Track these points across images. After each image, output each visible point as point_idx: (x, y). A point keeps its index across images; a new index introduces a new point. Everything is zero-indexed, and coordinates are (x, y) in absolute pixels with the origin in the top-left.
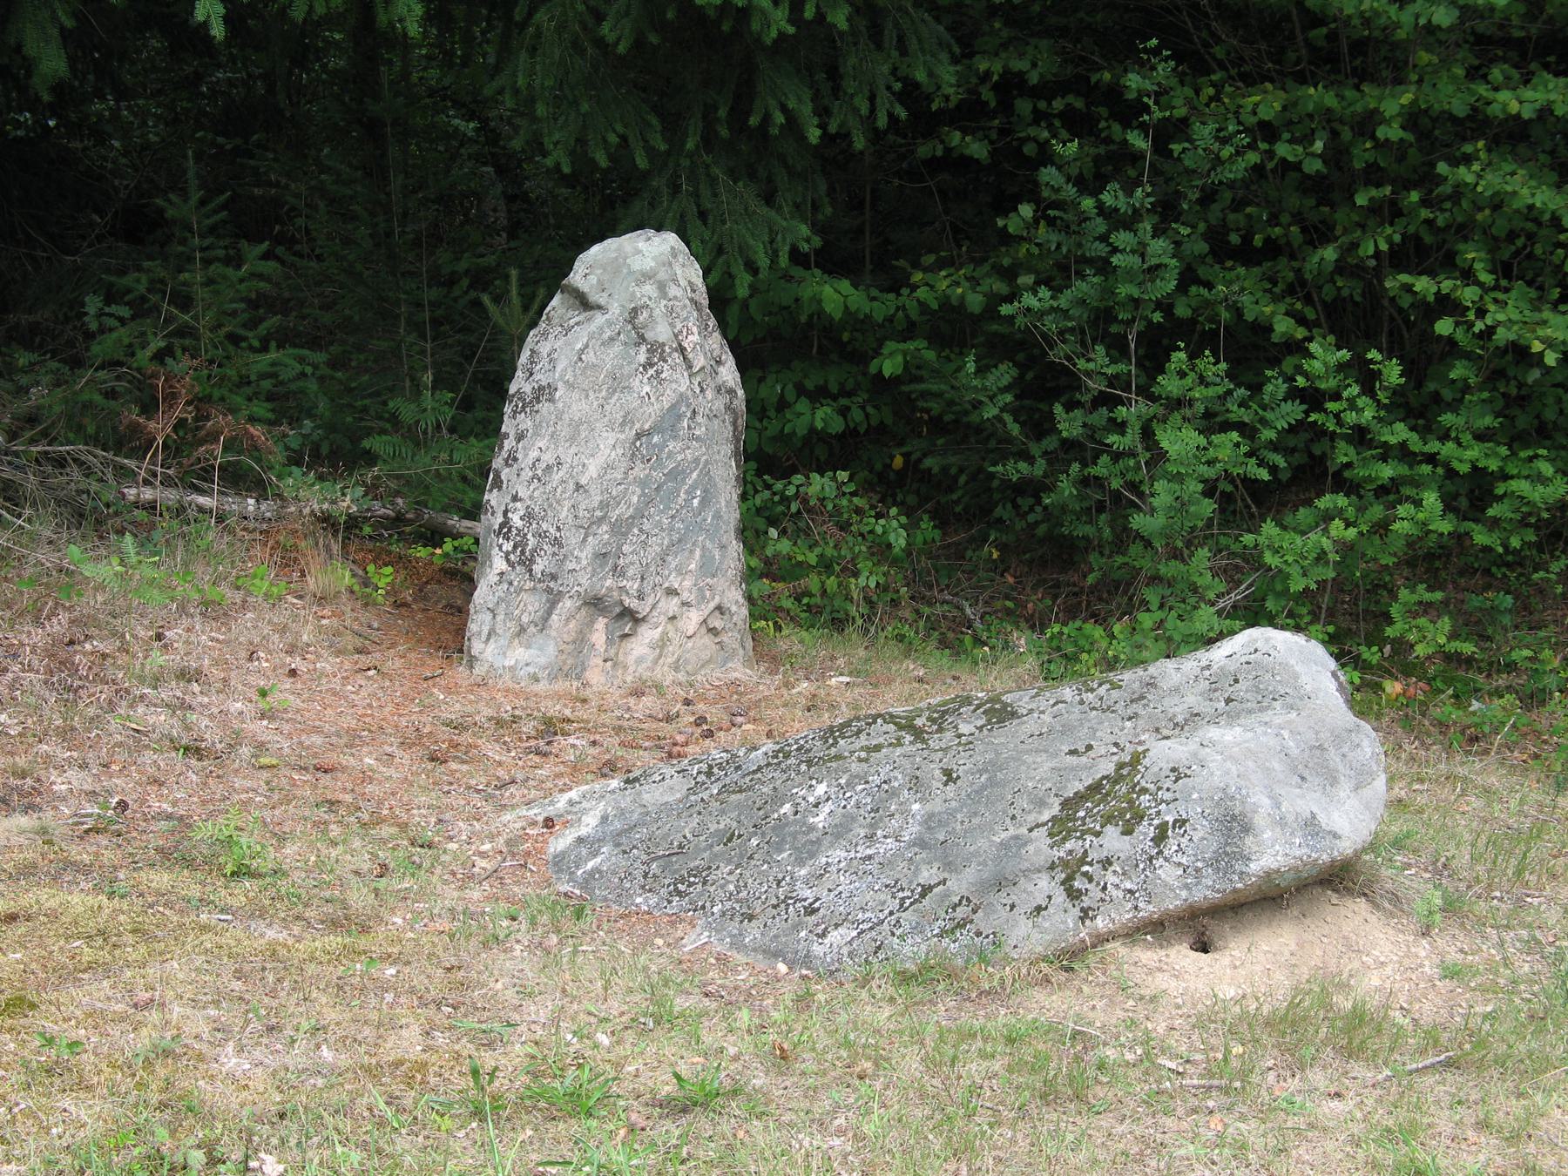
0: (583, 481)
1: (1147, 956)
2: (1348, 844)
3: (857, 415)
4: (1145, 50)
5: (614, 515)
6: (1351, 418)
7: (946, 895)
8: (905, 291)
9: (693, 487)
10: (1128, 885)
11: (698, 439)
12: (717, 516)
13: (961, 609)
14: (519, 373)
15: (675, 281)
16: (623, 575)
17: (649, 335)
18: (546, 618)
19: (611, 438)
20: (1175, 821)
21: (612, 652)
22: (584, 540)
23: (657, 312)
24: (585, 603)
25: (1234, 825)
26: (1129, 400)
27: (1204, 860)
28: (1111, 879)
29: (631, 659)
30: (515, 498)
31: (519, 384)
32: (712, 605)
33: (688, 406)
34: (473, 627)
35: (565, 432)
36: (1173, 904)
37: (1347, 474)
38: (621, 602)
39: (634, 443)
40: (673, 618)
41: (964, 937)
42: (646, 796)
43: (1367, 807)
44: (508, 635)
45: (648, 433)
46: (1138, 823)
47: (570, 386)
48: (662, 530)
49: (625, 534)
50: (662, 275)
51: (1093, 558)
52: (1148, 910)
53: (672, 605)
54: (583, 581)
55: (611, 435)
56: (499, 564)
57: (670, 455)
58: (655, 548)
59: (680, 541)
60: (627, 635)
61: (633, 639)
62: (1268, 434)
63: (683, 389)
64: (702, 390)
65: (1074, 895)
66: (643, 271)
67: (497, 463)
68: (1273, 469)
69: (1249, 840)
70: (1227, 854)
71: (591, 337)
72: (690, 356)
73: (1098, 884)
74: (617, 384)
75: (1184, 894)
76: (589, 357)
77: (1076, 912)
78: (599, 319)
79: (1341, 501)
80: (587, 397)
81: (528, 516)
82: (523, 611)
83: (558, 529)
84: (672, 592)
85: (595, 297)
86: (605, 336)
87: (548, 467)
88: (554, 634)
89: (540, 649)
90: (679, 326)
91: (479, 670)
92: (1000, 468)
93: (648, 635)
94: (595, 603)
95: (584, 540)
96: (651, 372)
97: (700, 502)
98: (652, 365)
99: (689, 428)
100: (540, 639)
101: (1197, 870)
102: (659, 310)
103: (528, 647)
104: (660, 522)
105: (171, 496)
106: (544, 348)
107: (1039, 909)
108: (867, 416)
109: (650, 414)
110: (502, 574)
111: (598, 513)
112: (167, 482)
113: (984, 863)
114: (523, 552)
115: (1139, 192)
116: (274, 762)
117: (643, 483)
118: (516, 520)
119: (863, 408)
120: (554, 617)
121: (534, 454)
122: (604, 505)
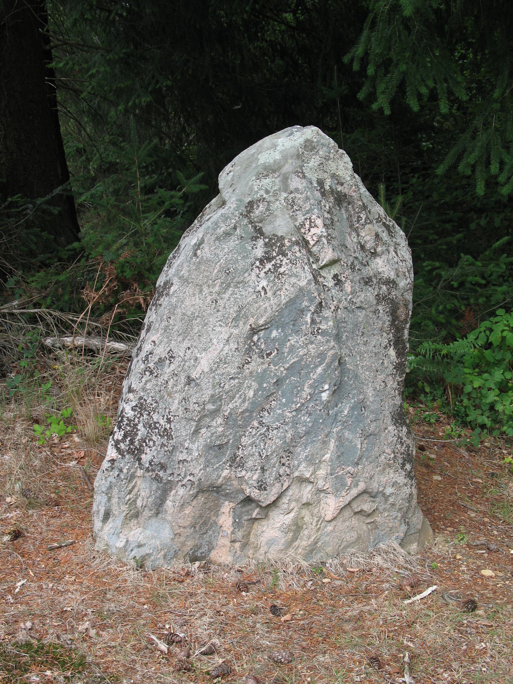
0: (194, 375)
5: (227, 409)
9: (321, 380)
11: (324, 333)
16: (241, 465)
17: (267, 229)
19: (224, 332)
21: (239, 535)
22: (196, 432)
23: (274, 206)
29: (263, 539)
32: (354, 492)
33: (311, 300)
38: (242, 491)
39: (250, 337)
45: (266, 327)
47: (185, 281)
48: (285, 423)
53: (306, 492)
57: (292, 349)
58: (276, 440)
61: (264, 523)
63: (303, 283)
71: (206, 233)
72: (315, 249)
74: (230, 278)
76: (205, 252)
80: (201, 291)
81: (140, 407)
83: (169, 421)
84: (302, 480)
86: (223, 228)
87: (161, 361)
88: (169, 518)
90: (301, 218)
91: (100, 546)
95: (196, 432)
96: (269, 266)
98: (269, 259)
99: (313, 321)
104: (282, 415)
109: (267, 308)
110: (113, 461)
111: (210, 407)
114: (132, 442)
117: (261, 378)
120: (169, 503)
122: (213, 399)
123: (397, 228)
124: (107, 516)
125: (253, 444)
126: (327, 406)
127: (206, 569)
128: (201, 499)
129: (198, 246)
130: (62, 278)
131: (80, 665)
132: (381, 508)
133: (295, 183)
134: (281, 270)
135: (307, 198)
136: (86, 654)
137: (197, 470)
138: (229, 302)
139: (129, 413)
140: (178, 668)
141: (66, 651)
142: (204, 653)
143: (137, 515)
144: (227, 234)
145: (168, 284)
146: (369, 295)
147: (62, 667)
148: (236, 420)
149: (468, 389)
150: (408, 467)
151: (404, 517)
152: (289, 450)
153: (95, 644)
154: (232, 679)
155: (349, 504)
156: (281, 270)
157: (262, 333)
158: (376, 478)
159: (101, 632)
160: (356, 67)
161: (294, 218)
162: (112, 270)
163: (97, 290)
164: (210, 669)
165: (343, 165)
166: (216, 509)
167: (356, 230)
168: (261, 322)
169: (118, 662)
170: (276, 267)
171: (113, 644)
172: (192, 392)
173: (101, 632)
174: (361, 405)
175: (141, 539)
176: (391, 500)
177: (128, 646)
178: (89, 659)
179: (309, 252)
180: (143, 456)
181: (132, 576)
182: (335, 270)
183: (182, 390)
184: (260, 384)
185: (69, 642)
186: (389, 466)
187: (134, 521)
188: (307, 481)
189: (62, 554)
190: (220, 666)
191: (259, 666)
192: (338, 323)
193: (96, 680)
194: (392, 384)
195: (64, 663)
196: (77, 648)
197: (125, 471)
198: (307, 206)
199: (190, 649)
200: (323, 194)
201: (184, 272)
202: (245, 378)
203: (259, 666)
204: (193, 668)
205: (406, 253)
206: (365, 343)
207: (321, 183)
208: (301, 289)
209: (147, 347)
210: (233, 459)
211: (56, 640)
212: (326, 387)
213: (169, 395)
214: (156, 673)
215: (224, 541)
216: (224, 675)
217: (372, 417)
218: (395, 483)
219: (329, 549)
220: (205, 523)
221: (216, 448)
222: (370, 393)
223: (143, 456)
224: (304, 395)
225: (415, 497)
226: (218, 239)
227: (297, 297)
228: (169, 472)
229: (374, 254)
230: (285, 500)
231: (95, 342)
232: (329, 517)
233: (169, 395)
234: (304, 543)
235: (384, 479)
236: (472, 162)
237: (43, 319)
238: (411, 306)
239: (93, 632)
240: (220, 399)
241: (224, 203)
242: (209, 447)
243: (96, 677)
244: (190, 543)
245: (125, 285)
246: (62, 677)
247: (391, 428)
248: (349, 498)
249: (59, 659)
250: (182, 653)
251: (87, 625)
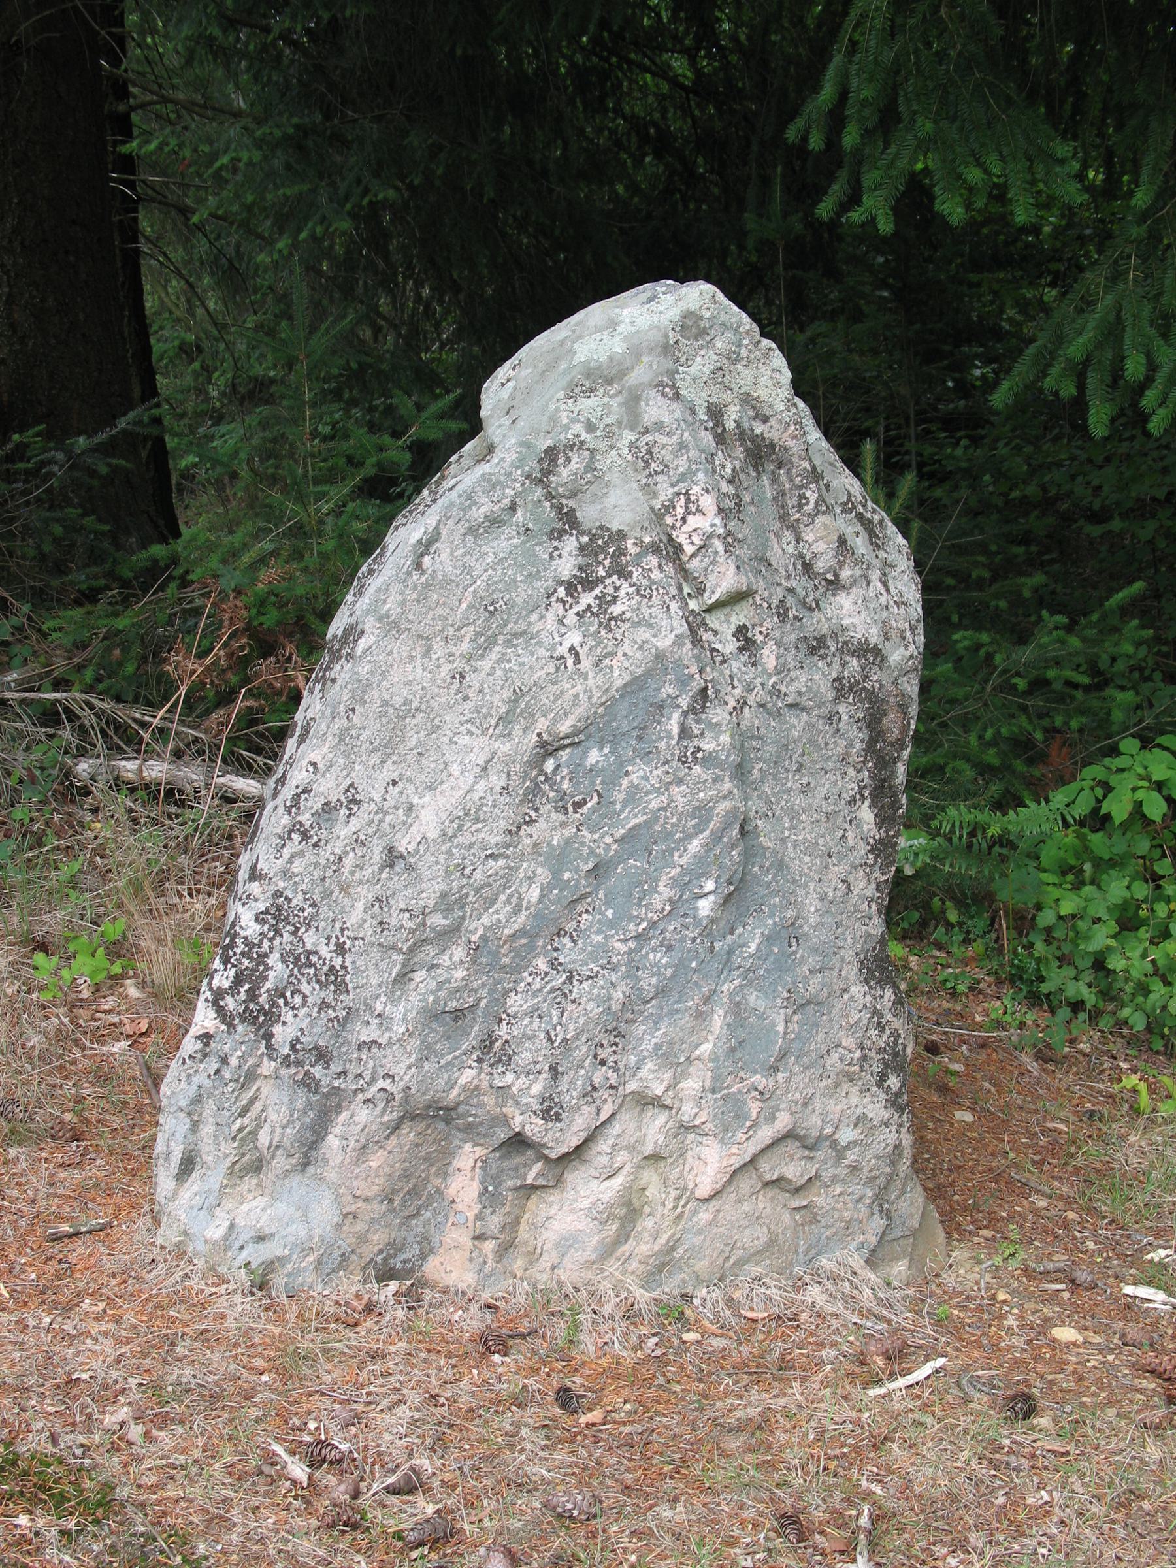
0: (403, 845)
5: (476, 928)
9: (699, 870)
16: (505, 1060)
17: (588, 514)
18: (314, 1145)
19: (477, 749)
21: (494, 1222)
22: (403, 977)
23: (602, 462)
24: (409, 1116)
29: (549, 1236)
32: (766, 1134)
33: (683, 682)
35: (372, 730)
38: (505, 1120)
40: (655, 1158)
45: (576, 740)
47: (392, 626)
48: (610, 966)
49: (515, 970)
53: (654, 1130)
55: (479, 742)
58: (586, 1006)
59: (661, 992)
61: (553, 1197)
63: (664, 642)
72: (695, 565)
74: (497, 623)
76: (442, 561)
80: (428, 651)
81: (276, 915)
83: (341, 950)
84: (645, 1102)
86: (484, 508)
88: (332, 1176)
91: (168, 1235)
93: (589, 1192)
95: (403, 977)
96: (587, 599)
98: (589, 583)
99: (685, 732)
110: (206, 1038)
111: (438, 920)
114: (252, 995)
117: (559, 858)
120: (333, 1141)
122: (446, 903)
123: (891, 528)
124: (188, 1165)
125: (534, 1012)
126: (709, 931)
127: (411, 1298)
128: (408, 1134)
129: (426, 546)
130: (122, 623)
131: (100, 1504)
132: (826, 1176)
133: (657, 409)
134: (616, 610)
135: (682, 446)
136: (116, 1481)
137: (402, 1067)
138: (492, 678)
139: (250, 927)
140: (329, 1520)
141: (70, 1471)
142: (393, 1490)
143: (257, 1167)
144: (494, 522)
145: (353, 633)
146: (817, 678)
147: (56, 1508)
148: (496, 955)
149: (1046, 918)
150: (893, 1082)
151: (879, 1198)
152: (616, 1029)
153: (140, 1459)
154: (454, 1552)
155: (753, 1161)
156: (616, 610)
157: (565, 755)
158: (817, 1103)
159: (155, 1432)
161: (649, 490)
162: (237, 611)
163: (202, 655)
164: (404, 1526)
165: (770, 375)
166: (442, 1160)
167: (794, 528)
168: (564, 728)
169: (191, 1501)
170: (604, 602)
171: (181, 1459)
172: (396, 883)
173: (155, 1432)
174: (789, 933)
175: (265, 1222)
176: (851, 1157)
177: (216, 1466)
178: (122, 1492)
179: (682, 570)
180: (277, 1029)
181: (238, 1308)
182: (741, 615)
184: (556, 873)
185: (78, 1452)
186: (850, 1078)
187: (250, 1181)
188: (657, 1103)
189: (79, 1250)
190: (427, 1521)
191: (519, 1525)
192: (743, 739)
193: (134, 1540)
195: (63, 1498)
196: (95, 1466)
197: (234, 1061)
198: (682, 465)
199: (362, 1479)
200: (720, 438)
201: (391, 606)
202: (522, 857)
203: (519, 1525)
204: (366, 1524)
206: (805, 790)
207: (716, 413)
208: (660, 656)
209: (298, 776)
210: (487, 1044)
211: (49, 1446)
212: (710, 885)
213: (345, 889)
214: (278, 1531)
215: (457, 1236)
216: (436, 1541)
217: (813, 961)
218: (862, 1117)
219: (701, 1266)
220: (414, 1192)
222: (811, 905)
223: (277, 1029)
224: (658, 901)
225: (907, 1153)
226: (471, 531)
227: (649, 673)
228: (336, 1068)
229: (834, 585)
230: (603, 1145)
231: (191, 774)
232: (703, 1191)
233: (345, 889)
234: (644, 1249)
235: (835, 1108)
237: (72, 716)
238: (914, 710)
239: (135, 1432)
240: (462, 902)
241: (491, 449)
242: (433, 1015)
243: (134, 1535)
244: (378, 1238)
245: (266, 646)
246: (54, 1532)
247: (858, 990)
248: (752, 1149)
249: (50, 1488)
250: (342, 1488)
251: (124, 1413)
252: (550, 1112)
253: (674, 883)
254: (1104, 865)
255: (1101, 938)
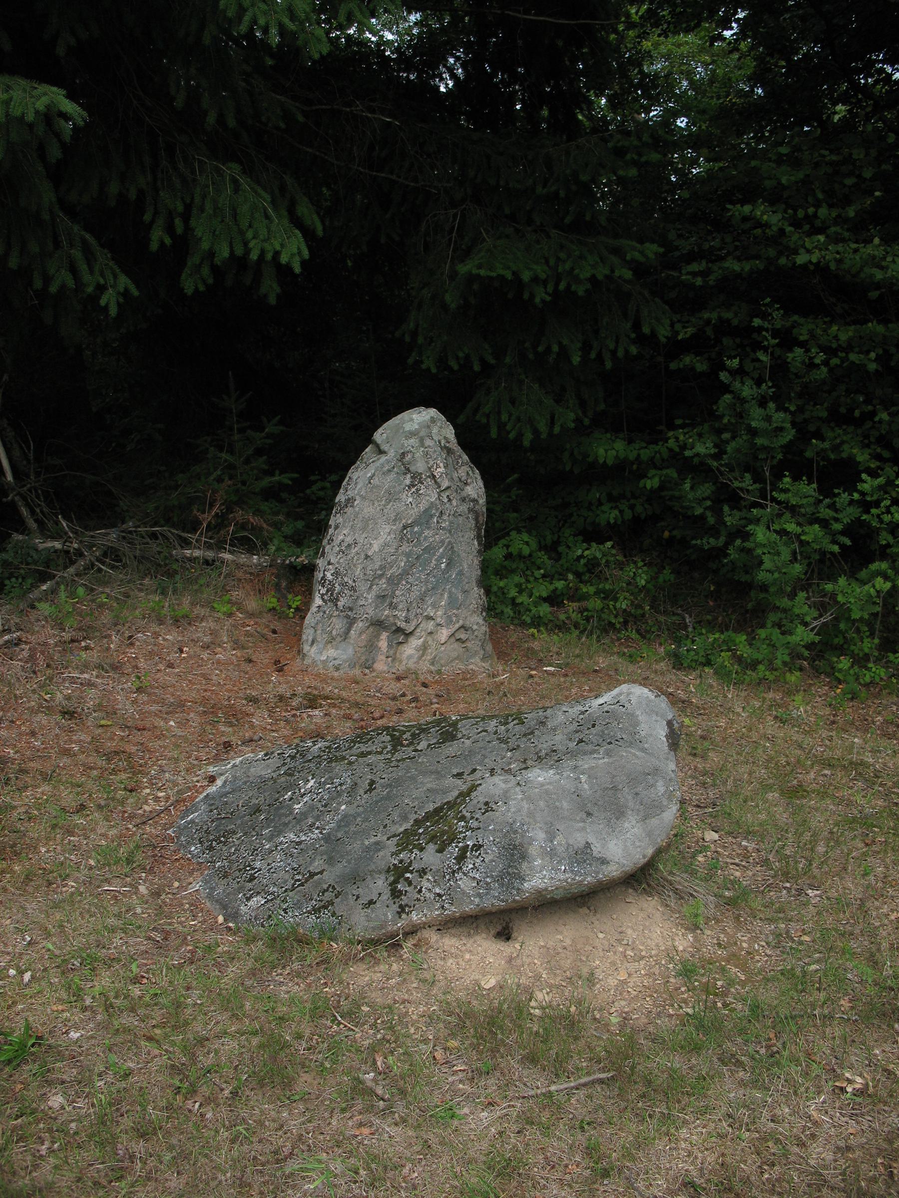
0: (370, 554)
1: (449, 942)
2: (614, 868)
3: (639, 509)
4: (765, 305)
5: (389, 573)
6: (887, 518)
7: (319, 883)
8: (661, 443)
9: (441, 557)
10: (438, 891)
12: (461, 573)
13: (684, 619)
14: (341, 491)
15: (430, 436)
16: (395, 608)
17: (412, 468)
20: (474, 845)
21: (391, 652)
22: (370, 587)
24: (372, 624)
25: (515, 853)
26: (767, 505)
27: (492, 877)
28: (426, 884)
29: (405, 656)
30: (329, 563)
31: (341, 497)
32: (457, 626)
33: (437, 509)
34: (304, 637)
36: (469, 908)
37: (888, 551)
38: (395, 624)
39: (402, 531)
40: (431, 633)
41: (325, 915)
42: (252, 770)
43: (649, 834)
44: (324, 642)
45: (411, 525)
46: (449, 844)
47: (363, 498)
48: (421, 582)
50: (422, 434)
51: (753, 593)
52: (452, 910)
53: (431, 625)
54: (370, 612)
56: (318, 601)
57: (426, 538)
58: (415, 593)
59: (433, 588)
60: (401, 643)
61: (405, 645)
62: (838, 527)
64: (450, 500)
65: (396, 894)
66: (418, 432)
67: (325, 542)
68: (842, 546)
69: (525, 865)
70: (509, 874)
73: (416, 887)
74: (391, 496)
75: (477, 900)
76: (376, 481)
77: (395, 908)
78: (383, 458)
79: (884, 566)
80: (373, 504)
81: (336, 574)
82: (333, 628)
83: (354, 581)
85: (384, 447)
86: (385, 469)
87: (349, 545)
88: (352, 642)
89: (344, 650)
92: (699, 542)
94: (378, 624)
95: (370, 587)
96: (413, 490)
97: (448, 565)
98: (414, 486)
99: (438, 522)
100: (343, 645)
101: (487, 884)
102: (419, 454)
103: (337, 649)
105: (210, 554)
106: (355, 478)
107: (371, 902)
108: (645, 509)
109: (414, 513)
110: (319, 607)
111: (379, 572)
112: (209, 547)
113: (349, 862)
114: (332, 595)
115: (764, 386)
116: (109, 723)
117: (408, 555)
118: (329, 576)
119: (643, 505)
121: (341, 537)
122: (382, 568)
124: (313, 642)
128: (371, 629)
133: (428, 442)
134: (421, 492)
135: (435, 451)
137: (371, 611)
143: (333, 639)
145: (350, 501)
146: (464, 508)
148: (393, 580)
150: (484, 614)
160: (407, 339)
161: (427, 462)
165: (449, 432)
166: (377, 636)
167: (456, 469)
168: (409, 522)
174: (461, 573)
176: (476, 633)
179: (436, 482)
180: (339, 603)
183: (363, 562)
187: (330, 645)
188: (431, 618)
194: (476, 562)
205: (481, 483)
206: (463, 536)
208: (432, 503)
213: (354, 565)
219: (442, 662)
220: (372, 645)
221: (382, 597)
223: (339, 603)
226: (384, 473)
227: (430, 508)
229: (466, 484)
233: (354, 565)
234: (429, 657)
236: (487, 412)
240: (385, 567)
242: (378, 597)
244: (363, 658)
247: (476, 589)
248: (454, 630)
252: (407, 621)
253: (436, 560)
254: (513, 571)
255: (513, 593)
